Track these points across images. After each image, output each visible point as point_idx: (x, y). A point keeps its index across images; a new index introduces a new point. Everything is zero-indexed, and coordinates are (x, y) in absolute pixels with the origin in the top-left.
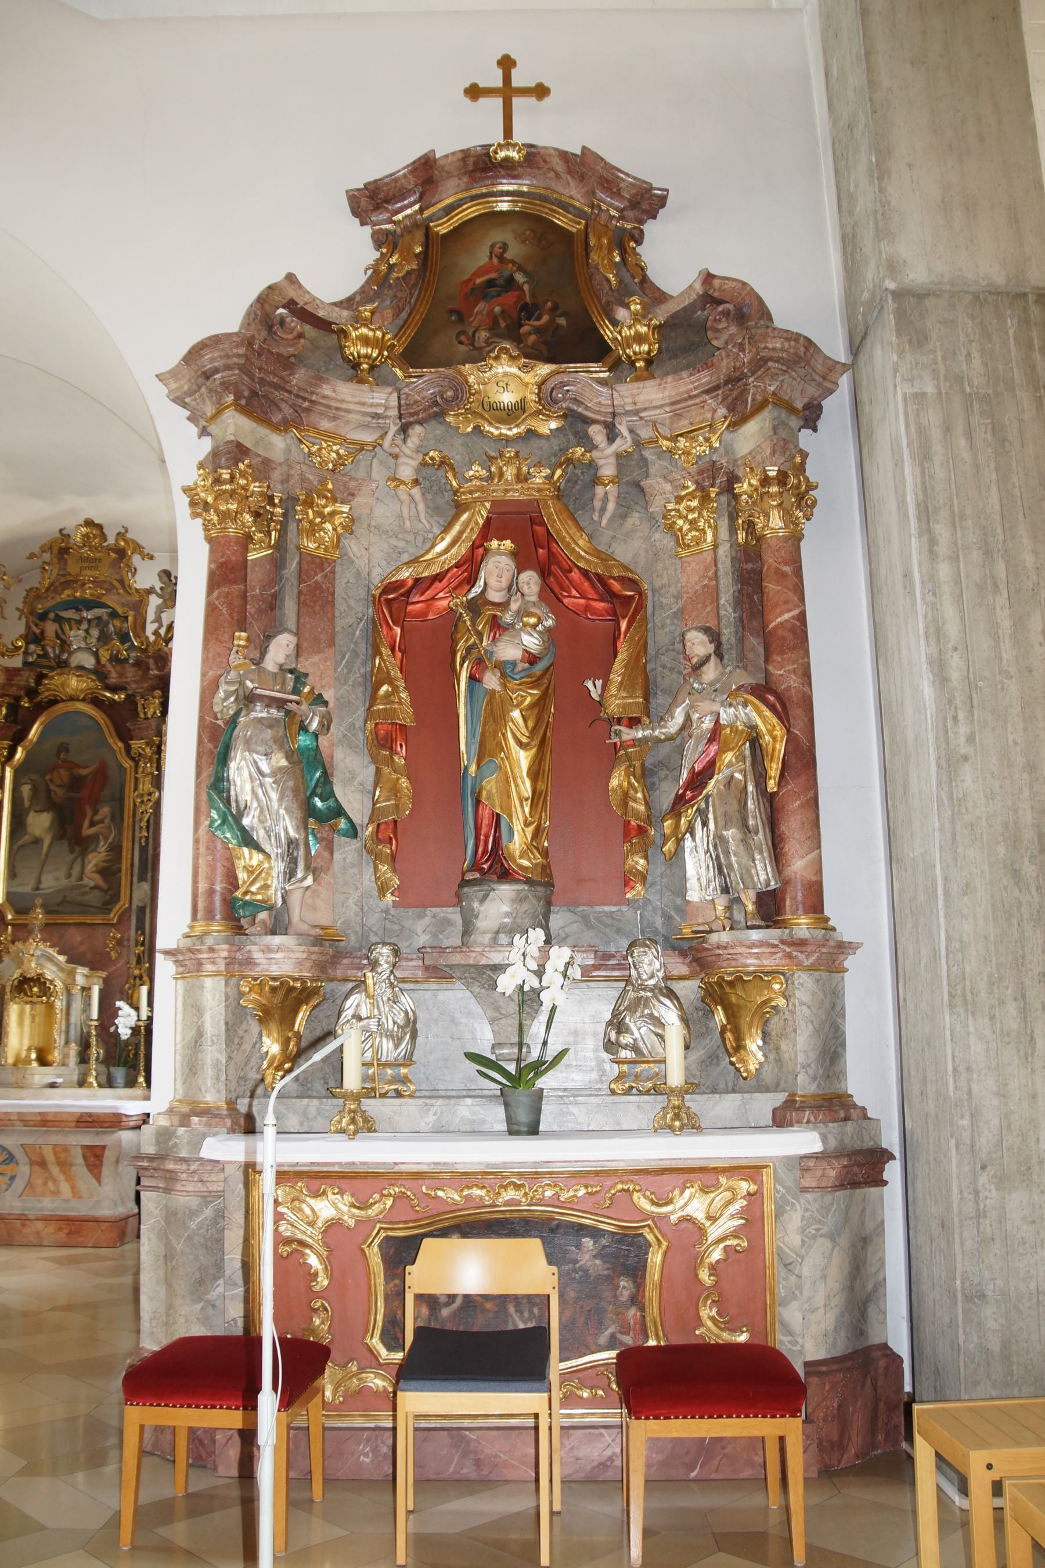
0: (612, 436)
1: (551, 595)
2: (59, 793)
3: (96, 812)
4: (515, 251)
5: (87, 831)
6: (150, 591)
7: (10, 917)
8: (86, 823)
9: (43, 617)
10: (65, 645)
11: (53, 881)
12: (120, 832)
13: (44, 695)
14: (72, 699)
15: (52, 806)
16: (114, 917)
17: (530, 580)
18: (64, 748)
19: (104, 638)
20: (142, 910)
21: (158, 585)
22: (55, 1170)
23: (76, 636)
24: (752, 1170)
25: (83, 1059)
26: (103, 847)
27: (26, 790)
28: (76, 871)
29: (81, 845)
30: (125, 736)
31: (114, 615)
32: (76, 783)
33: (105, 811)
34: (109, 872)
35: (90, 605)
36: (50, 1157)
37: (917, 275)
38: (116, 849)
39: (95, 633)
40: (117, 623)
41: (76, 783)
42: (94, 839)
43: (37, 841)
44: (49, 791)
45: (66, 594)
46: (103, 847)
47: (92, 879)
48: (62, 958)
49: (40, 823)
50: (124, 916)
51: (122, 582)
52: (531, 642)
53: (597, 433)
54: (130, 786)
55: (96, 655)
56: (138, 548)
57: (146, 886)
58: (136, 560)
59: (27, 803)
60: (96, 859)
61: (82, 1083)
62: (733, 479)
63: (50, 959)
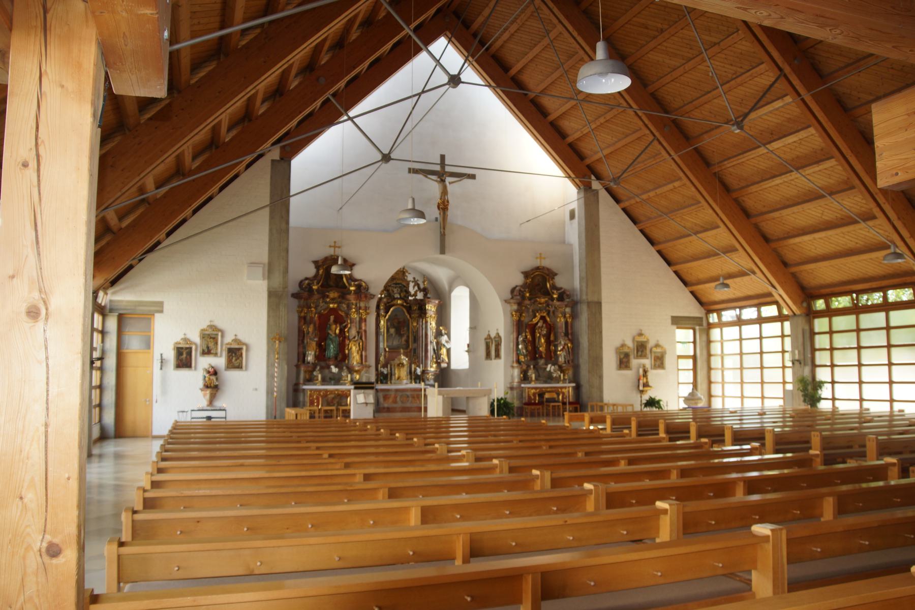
0: (552, 307)
1: (546, 327)
2: (396, 324)
3: (403, 328)
4: (540, 280)
5: (402, 333)
6: (410, 281)
7: (387, 349)
8: (402, 331)
9: (389, 286)
10: (393, 291)
11: (396, 343)
12: (409, 333)
13: (392, 303)
14: (398, 304)
15: (394, 327)
16: (409, 350)
17: (544, 325)
18: (396, 315)
19: (401, 291)
20: (415, 350)
21: (412, 280)
22: (416, 398)
23: (395, 290)
24: (569, 387)
25: (411, 379)
26: (405, 336)
27: (389, 324)
28: (400, 341)
29: (401, 335)
30: (409, 313)
31: (404, 286)
32: (399, 322)
33: (405, 329)
34: (407, 341)
35: (399, 284)
36: (415, 396)
37: (590, 300)
38: (408, 337)
39: (399, 290)
40: (405, 288)
41: (399, 322)
42: (404, 335)
43: (392, 335)
44: (393, 324)
45: (395, 282)
46: (405, 336)
47: (404, 342)
48: (407, 359)
49: (392, 331)
50: (411, 350)
51: (404, 278)
52: (545, 332)
53: (550, 307)
54: (410, 324)
55: (400, 294)
56: (407, 272)
57: (415, 345)
58: (407, 274)
59: (389, 326)
60: (404, 339)
61: (411, 383)
62: (565, 314)
63: (405, 359)
